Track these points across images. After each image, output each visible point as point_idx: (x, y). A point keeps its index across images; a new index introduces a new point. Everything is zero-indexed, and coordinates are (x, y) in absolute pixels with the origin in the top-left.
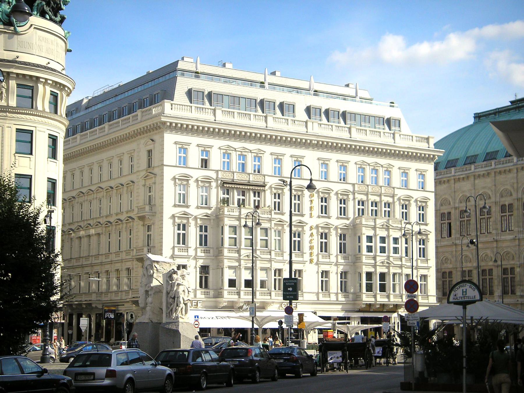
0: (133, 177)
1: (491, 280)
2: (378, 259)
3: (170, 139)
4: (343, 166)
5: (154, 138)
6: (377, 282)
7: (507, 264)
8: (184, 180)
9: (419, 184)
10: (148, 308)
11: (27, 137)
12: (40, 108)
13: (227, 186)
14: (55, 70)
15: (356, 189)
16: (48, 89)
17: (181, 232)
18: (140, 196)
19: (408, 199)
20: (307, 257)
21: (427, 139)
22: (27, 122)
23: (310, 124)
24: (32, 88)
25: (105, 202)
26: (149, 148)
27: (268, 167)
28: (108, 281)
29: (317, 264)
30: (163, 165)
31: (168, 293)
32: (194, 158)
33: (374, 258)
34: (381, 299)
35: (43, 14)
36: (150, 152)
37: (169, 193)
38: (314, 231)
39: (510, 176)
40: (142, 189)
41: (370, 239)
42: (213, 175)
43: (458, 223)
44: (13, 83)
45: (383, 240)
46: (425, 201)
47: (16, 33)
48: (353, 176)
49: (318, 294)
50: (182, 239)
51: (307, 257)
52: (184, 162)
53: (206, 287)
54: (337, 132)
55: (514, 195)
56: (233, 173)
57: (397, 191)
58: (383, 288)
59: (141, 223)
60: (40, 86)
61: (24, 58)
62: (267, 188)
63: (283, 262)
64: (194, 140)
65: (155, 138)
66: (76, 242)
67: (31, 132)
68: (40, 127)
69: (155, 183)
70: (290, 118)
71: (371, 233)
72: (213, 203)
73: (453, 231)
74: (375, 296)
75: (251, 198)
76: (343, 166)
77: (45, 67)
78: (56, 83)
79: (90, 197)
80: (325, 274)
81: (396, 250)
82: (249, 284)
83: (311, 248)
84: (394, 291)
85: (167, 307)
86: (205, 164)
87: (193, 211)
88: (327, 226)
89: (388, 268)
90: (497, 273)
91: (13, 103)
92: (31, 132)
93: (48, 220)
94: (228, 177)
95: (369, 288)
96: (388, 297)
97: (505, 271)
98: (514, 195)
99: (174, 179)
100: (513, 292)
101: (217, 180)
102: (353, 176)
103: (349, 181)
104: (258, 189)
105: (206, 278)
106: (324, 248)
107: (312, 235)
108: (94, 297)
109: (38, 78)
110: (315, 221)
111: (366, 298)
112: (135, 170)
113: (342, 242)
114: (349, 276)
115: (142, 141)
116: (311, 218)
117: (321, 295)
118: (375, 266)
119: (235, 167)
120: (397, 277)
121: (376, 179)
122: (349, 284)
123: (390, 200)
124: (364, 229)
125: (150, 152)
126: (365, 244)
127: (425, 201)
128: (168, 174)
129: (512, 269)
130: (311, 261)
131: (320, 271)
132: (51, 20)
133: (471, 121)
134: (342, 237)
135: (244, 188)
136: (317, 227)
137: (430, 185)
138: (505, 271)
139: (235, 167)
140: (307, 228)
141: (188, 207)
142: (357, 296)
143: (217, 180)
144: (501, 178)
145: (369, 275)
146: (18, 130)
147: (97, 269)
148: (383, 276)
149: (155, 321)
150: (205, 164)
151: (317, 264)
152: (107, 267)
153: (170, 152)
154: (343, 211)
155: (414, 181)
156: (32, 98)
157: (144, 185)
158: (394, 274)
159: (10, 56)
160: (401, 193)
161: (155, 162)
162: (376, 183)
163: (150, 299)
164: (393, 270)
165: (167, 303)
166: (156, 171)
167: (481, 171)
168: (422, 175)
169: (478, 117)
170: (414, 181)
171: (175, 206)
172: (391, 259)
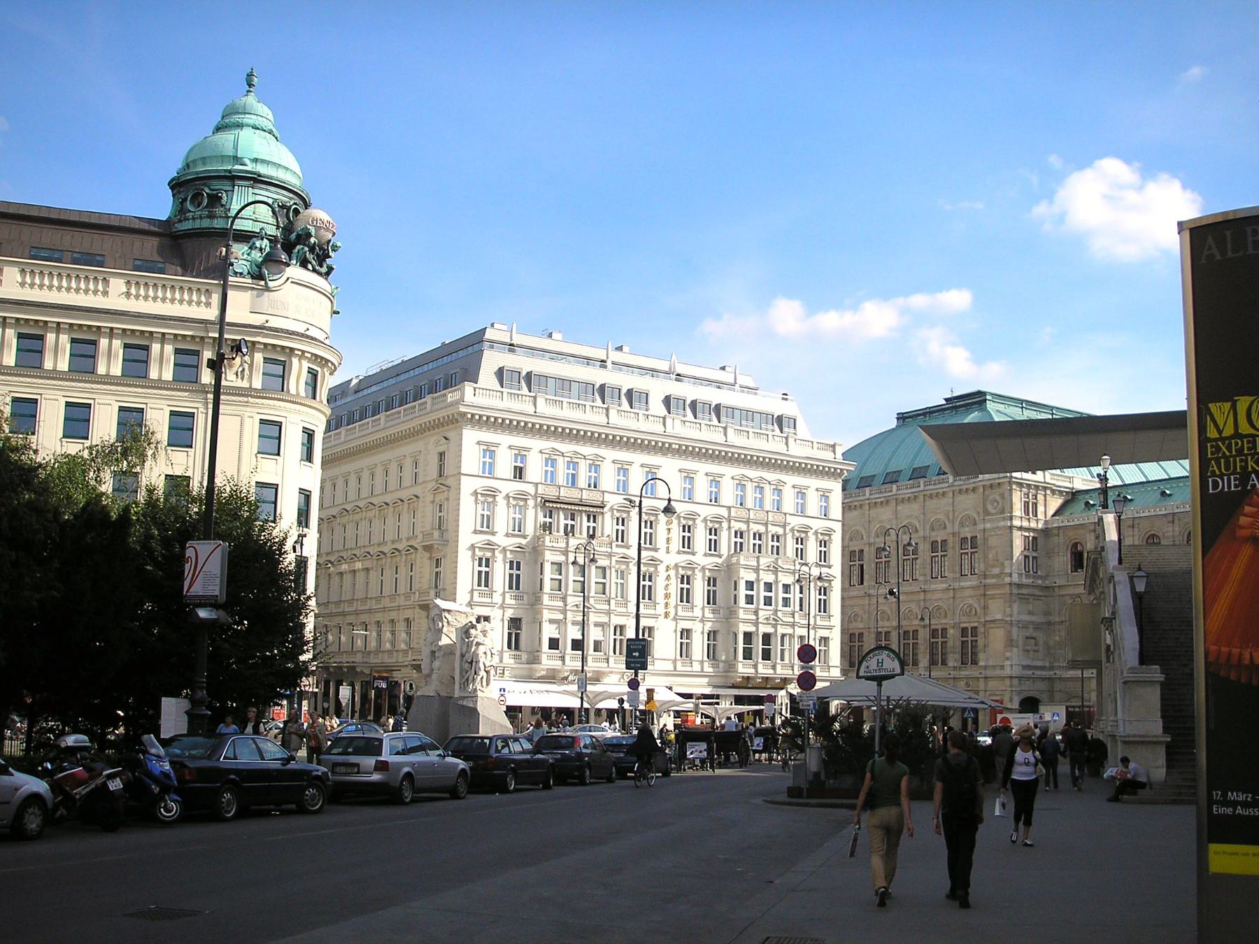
0: (418, 490)
2: (761, 613)
3: (471, 437)
4: (715, 481)
5: (449, 435)
6: (758, 646)
7: (937, 623)
8: (489, 496)
9: (821, 508)
10: (434, 676)
11: (274, 431)
12: (293, 391)
13: (549, 505)
14: (315, 339)
15: (733, 514)
16: (306, 365)
17: (484, 569)
18: (426, 517)
19: (805, 530)
20: (660, 609)
21: (834, 446)
22: (274, 409)
23: (669, 421)
24: (283, 364)
25: (377, 524)
26: (441, 449)
27: (608, 479)
28: (379, 635)
29: (675, 619)
30: (460, 474)
31: (463, 656)
32: (504, 466)
33: (756, 613)
34: (764, 670)
35: (304, 263)
36: (442, 455)
37: (468, 514)
38: (672, 573)
40: (429, 508)
41: (750, 585)
42: (530, 489)
43: (873, 565)
44: (259, 357)
45: (768, 587)
46: (829, 533)
47: (267, 289)
48: (728, 495)
49: (675, 661)
50: (484, 580)
51: (660, 609)
52: (489, 470)
53: (517, 648)
54: (707, 433)
55: (949, 529)
56: (559, 487)
57: (789, 519)
58: (767, 655)
59: (427, 555)
60: (295, 361)
61: (275, 322)
62: (606, 509)
63: (627, 615)
64: (504, 440)
65: (450, 435)
66: (336, 579)
67: (279, 425)
69: (448, 499)
70: (641, 412)
71: (751, 577)
72: (530, 529)
73: (866, 577)
74: (755, 667)
75: (584, 523)
76: (715, 481)
77: (303, 335)
78: (316, 356)
79: (357, 517)
80: (686, 633)
81: (786, 602)
82: (578, 645)
83: (667, 596)
84: (782, 659)
85: (462, 676)
86: (519, 473)
87: (500, 540)
88: (691, 566)
89: (775, 626)
90: (924, 635)
91: (257, 383)
92: (279, 425)
93: (298, 547)
94: (551, 493)
95: (748, 655)
96: (774, 667)
97: (934, 633)
98: (949, 529)
99: (475, 493)
100: (944, 663)
101: (535, 497)
102: (728, 495)
103: (723, 501)
104: (594, 511)
105: (517, 635)
106: (686, 596)
107: (668, 578)
108: (358, 658)
109: (292, 350)
110: (673, 558)
111: (743, 669)
112: (420, 480)
113: (712, 588)
114: (719, 637)
115: (432, 440)
116: (668, 554)
117: (679, 664)
118: (756, 624)
119: (561, 479)
120: (787, 639)
121: (761, 500)
122: (719, 648)
123: (780, 531)
124: (742, 570)
125: (442, 455)
126: (743, 591)
127: (829, 533)
128: (468, 486)
129: (944, 630)
131: (679, 630)
132: (314, 270)
133: (893, 424)
134: (712, 582)
135: (574, 508)
136: (676, 566)
137: (836, 511)
138: (934, 633)
139: (561, 479)
140: (662, 568)
141: (493, 534)
142: (731, 666)
143: (535, 497)
144: (932, 504)
145: (748, 636)
146: (262, 422)
147: (364, 618)
148: (767, 638)
149: (443, 694)
150: (519, 473)
152: (379, 617)
153: (470, 458)
154: (713, 546)
155: (813, 506)
156: (283, 377)
157: (433, 502)
158: (783, 636)
159: (257, 320)
160: (794, 522)
161: (449, 470)
162: (761, 506)
163: (437, 664)
164: (781, 630)
165: (461, 670)
166: (449, 482)
167: (906, 493)
168: (825, 495)
169: (902, 417)
170: (813, 506)
171: (475, 532)
172: (780, 614)
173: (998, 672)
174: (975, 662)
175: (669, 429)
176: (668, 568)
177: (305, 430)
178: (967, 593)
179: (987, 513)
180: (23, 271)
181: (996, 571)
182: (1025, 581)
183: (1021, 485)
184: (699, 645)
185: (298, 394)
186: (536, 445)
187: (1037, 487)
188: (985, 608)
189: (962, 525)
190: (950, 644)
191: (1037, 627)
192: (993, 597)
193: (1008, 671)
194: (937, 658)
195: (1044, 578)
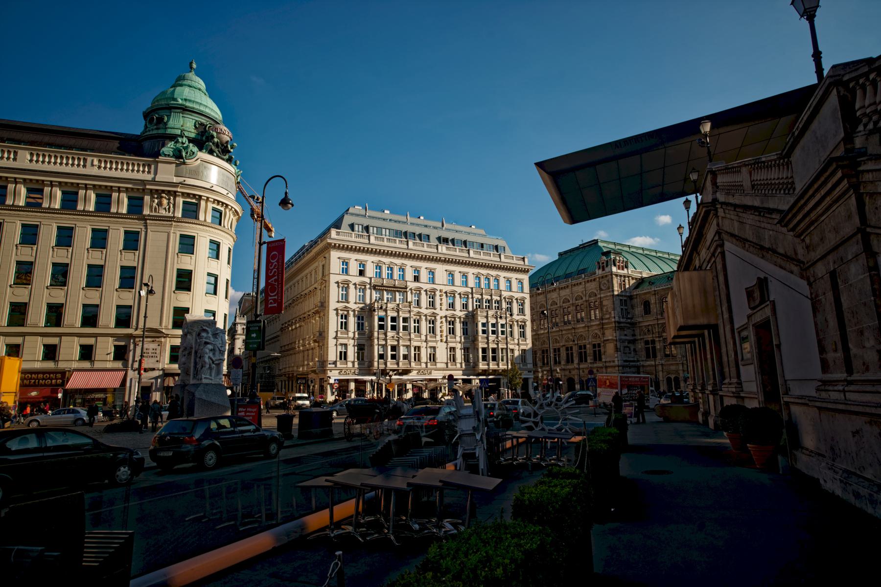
0: (316, 286)
1: (572, 354)
3: (335, 255)
7: (581, 343)
8: (345, 286)
9: (517, 288)
16: (211, 206)
19: (511, 298)
20: (438, 338)
21: (523, 259)
22: (190, 229)
23: (440, 247)
29: (446, 342)
32: (354, 268)
34: (493, 366)
37: (334, 293)
38: (444, 320)
39: (581, 287)
42: (368, 281)
46: (523, 299)
48: (472, 282)
49: (447, 364)
50: (345, 326)
51: (438, 338)
52: (346, 271)
54: (458, 253)
55: (584, 299)
58: (494, 359)
60: (203, 203)
64: (353, 257)
65: (327, 256)
67: (193, 237)
68: (201, 233)
70: (425, 243)
74: (488, 365)
76: (465, 275)
82: (405, 357)
83: (441, 331)
84: (502, 360)
86: (362, 273)
87: (352, 305)
88: (454, 317)
90: (575, 349)
92: (193, 237)
96: (498, 365)
97: (580, 347)
98: (584, 299)
99: (337, 283)
100: (586, 361)
101: (370, 284)
102: (472, 282)
105: (363, 354)
106: (452, 331)
107: (441, 322)
109: (200, 196)
110: (443, 313)
111: (482, 366)
116: (442, 311)
120: (504, 351)
126: (480, 328)
127: (523, 299)
128: (333, 279)
129: (585, 346)
130: (441, 341)
133: (557, 258)
134: (464, 323)
136: (446, 317)
137: (527, 288)
138: (580, 347)
139: (384, 275)
140: (438, 318)
141: (348, 303)
142: (476, 364)
143: (370, 284)
144: (575, 289)
145: (484, 350)
146: (182, 236)
148: (494, 350)
150: (362, 273)
151: (446, 342)
153: (335, 265)
155: (515, 285)
158: (502, 349)
160: (505, 294)
161: (326, 273)
164: (500, 346)
166: (326, 279)
167: (563, 285)
168: (521, 282)
169: (560, 254)
170: (515, 285)
171: (338, 302)
173: (612, 364)
174: (600, 359)
175: (440, 251)
176: (441, 318)
177: (212, 242)
178: (594, 328)
179: (601, 289)
180: (32, 155)
181: (607, 316)
182: (622, 320)
183: (617, 275)
184: (459, 354)
185: (205, 220)
186: (370, 259)
187: (625, 277)
188: (603, 334)
189: (590, 297)
190: (588, 352)
191: (630, 342)
192: (607, 329)
193: (616, 363)
194: (582, 358)
195: (632, 318)
